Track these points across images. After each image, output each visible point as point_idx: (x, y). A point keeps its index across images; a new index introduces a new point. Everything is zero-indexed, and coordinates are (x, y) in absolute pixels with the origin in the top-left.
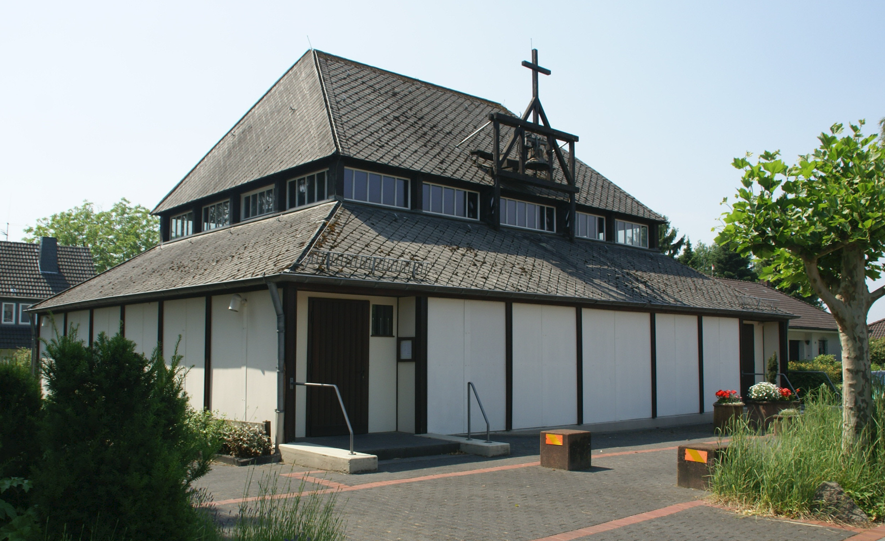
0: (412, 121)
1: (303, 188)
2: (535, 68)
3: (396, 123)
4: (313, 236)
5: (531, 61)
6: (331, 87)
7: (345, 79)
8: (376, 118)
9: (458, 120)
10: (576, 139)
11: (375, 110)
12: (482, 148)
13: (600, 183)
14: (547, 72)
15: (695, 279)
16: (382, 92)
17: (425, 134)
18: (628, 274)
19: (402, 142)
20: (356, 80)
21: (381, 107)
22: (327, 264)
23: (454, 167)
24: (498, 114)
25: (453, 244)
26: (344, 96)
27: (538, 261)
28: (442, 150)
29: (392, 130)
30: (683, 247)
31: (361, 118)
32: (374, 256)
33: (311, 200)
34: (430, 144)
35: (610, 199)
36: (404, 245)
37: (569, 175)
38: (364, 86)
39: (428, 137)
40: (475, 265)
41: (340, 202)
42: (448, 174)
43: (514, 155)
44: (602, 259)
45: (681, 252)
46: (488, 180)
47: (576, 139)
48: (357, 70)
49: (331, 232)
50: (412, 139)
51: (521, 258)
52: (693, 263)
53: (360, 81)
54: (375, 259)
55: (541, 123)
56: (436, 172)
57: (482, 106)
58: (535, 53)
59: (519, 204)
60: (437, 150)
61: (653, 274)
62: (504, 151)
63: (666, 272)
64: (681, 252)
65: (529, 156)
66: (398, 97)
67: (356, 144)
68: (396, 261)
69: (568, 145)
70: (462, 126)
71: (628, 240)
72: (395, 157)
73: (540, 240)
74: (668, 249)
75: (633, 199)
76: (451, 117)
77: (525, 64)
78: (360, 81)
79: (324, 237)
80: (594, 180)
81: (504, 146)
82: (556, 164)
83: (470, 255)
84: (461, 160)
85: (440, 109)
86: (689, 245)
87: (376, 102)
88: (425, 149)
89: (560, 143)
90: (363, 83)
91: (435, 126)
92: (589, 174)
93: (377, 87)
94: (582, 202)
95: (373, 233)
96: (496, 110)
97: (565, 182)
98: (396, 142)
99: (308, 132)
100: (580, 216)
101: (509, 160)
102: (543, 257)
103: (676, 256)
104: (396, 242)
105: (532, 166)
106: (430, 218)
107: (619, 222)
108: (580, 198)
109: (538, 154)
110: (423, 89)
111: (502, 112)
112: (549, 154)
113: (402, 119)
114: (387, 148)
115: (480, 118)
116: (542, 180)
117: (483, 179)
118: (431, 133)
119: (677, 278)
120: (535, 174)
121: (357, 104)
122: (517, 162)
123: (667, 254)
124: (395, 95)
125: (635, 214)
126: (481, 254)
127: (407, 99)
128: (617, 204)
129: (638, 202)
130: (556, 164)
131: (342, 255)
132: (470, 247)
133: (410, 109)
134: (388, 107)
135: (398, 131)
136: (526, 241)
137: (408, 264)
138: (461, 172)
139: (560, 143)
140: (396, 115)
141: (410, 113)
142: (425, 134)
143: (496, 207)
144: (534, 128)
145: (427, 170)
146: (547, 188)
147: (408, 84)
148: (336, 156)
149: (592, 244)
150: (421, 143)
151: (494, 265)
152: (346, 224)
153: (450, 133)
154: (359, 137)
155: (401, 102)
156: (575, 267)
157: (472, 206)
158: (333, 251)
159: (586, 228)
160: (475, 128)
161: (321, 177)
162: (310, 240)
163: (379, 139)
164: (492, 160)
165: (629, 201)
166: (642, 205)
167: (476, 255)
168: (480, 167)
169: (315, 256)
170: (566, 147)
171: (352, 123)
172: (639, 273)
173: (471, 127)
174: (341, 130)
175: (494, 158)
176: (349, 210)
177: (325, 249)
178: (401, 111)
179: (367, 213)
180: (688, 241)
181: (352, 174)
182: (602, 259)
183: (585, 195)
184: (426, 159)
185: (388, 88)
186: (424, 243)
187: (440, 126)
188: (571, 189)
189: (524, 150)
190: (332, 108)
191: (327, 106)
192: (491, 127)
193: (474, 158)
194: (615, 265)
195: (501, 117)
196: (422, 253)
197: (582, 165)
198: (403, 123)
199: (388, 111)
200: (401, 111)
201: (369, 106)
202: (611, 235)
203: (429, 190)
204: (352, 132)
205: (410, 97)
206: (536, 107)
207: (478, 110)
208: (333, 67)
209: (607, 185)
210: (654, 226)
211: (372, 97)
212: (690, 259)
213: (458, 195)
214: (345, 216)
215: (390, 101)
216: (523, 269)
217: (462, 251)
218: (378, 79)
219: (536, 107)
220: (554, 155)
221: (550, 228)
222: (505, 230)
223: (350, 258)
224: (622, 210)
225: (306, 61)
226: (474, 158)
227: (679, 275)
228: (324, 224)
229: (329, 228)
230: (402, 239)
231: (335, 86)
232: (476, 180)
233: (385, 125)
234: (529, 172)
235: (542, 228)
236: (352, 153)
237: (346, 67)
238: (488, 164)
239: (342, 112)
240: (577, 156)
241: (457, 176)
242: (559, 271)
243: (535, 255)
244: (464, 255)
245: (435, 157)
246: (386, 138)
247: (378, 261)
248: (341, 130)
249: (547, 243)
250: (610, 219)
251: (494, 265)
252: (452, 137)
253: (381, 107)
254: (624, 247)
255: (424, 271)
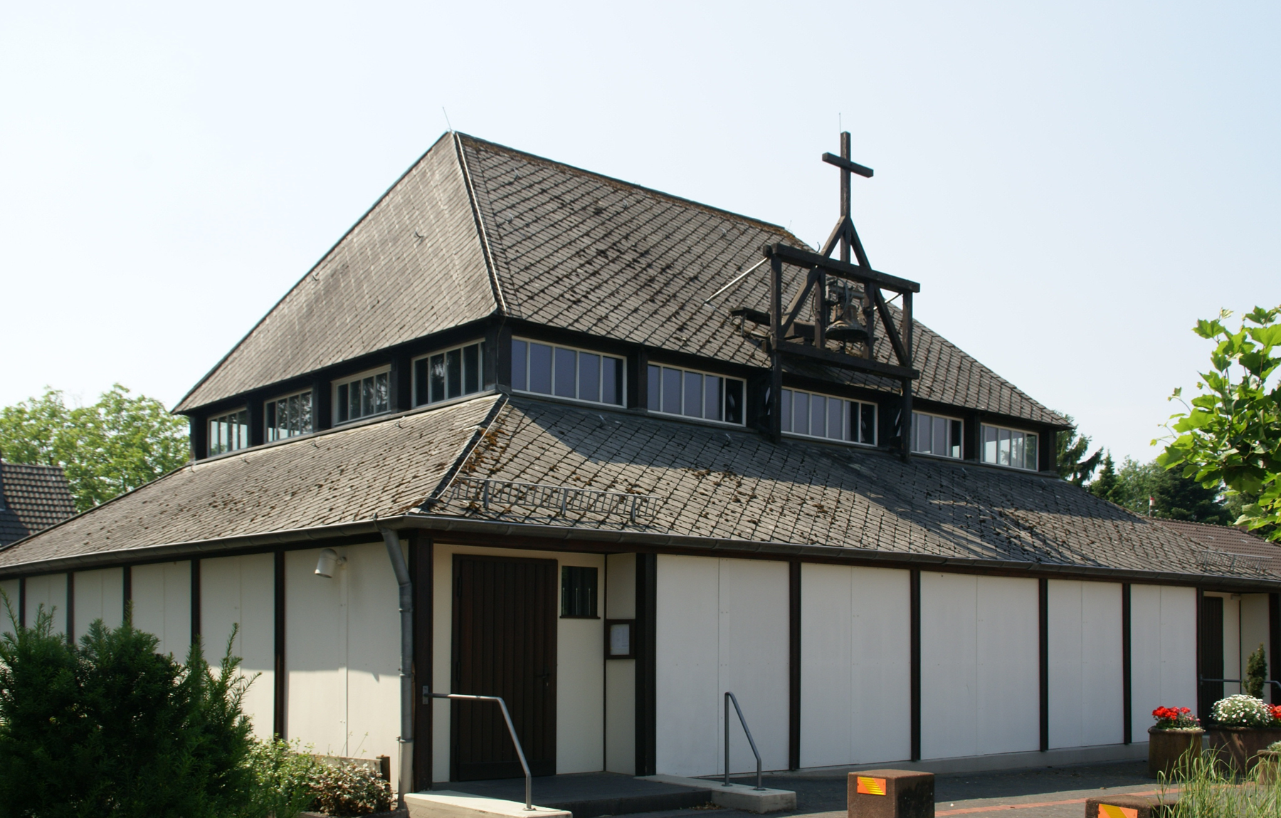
0: (628, 257)
1: (442, 371)
2: (846, 165)
3: (600, 261)
4: (459, 453)
5: (838, 153)
6: (486, 199)
7: (510, 184)
8: (566, 253)
9: (710, 255)
10: (916, 287)
11: (565, 239)
12: (751, 304)
13: (956, 362)
14: (867, 173)
15: (1119, 522)
16: (577, 207)
17: (652, 280)
18: (1001, 514)
19: (612, 294)
20: (531, 186)
21: (575, 234)
22: (484, 499)
23: (703, 337)
24: (779, 246)
25: (701, 466)
26: (510, 214)
27: (846, 494)
28: (682, 308)
29: (594, 274)
30: (1100, 468)
31: (540, 253)
32: (565, 486)
33: (455, 392)
34: (660, 297)
35: (973, 390)
36: (615, 467)
37: (903, 350)
38: (545, 198)
39: (656, 286)
40: (738, 501)
41: (504, 395)
42: (692, 349)
43: (807, 316)
44: (956, 490)
45: (1096, 476)
46: (762, 359)
47: (916, 287)
48: (531, 169)
49: (491, 445)
50: (629, 289)
51: (816, 489)
52: (1117, 494)
53: (537, 188)
54: (566, 491)
55: (854, 261)
56: (671, 346)
57: (751, 231)
58: (846, 139)
59: (814, 399)
60: (673, 307)
61: (1045, 515)
62: (790, 309)
63: (1069, 511)
64: (1096, 476)
65: (833, 317)
66: (605, 215)
67: (531, 298)
68: (603, 495)
69: (901, 298)
70: (716, 266)
71: (1002, 456)
72: (599, 320)
73: (850, 459)
74: (1072, 470)
75: (1013, 389)
76: (698, 250)
77: (829, 158)
78: (537, 188)
79: (479, 455)
80: (945, 358)
81: (789, 301)
82: (880, 331)
83: (730, 484)
84: (714, 325)
85: (678, 236)
86: (1109, 463)
87: (565, 224)
88: (651, 307)
89: (887, 295)
90: (544, 191)
91: (668, 267)
92: (936, 347)
93: (568, 198)
94: (923, 394)
95: (563, 448)
96: (775, 240)
97: (894, 361)
98: (601, 293)
99: (447, 276)
100: (920, 420)
101: (797, 325)
102: (854, 488)
103: (1086, 483)
104: (602, 463)
105: (836, 334)
106: (660, 423)
107: (986, 428)
108: (920, 388)
109: (848, 313)
110: (648, 202)
111: (786, 243)
112: (868, 313)
113: (612, 254)
114: (586, 304)
115: (747, 252)
116: (855, 357)
117: (752, 356)
118: (662, 279)
119: (1088, 521)
120: (843, 348)
121: (534, 228)
122: (812, 327)
123: (1070, 478)
124: (598, 212)
125: (1015, 413)
126: (748, 483)
127: (620, 220)
128: (984, 398)
129: (1021, 395)
130: (880, 331)
131: (509, 485)
132: (729, 471)
133: (626, 238)
134: (587, 234)
135: (605, 275)
136: (825, 461)
137: (623, 499)
138: (715, 345)
139: (887, 295)
140: (602, 247)
141: (626, 244)
142: (652, 280)
143: (775, 405)
144: (842, 269)
145: (655, 341)
146: (863, 371)
147: (621, 194)
148: (497, 317)
149: (939, 465)
150: (644, 295)
151: (770, 500)
152: (515, 433)
153: (696, 278)
154: (537, 285)
155: (610, 225)
156: (910, 504)
157: (733, 402)
158: (494, 477)
159: (930, 438)
160: (739, 269)
161: (471, 352)
162: (454, 460)
163: (572, 289)
164: (768, 324)
165: (1006, 392)
166: (1028, 399)
167: (739, 485)
168: (747, 336)
169: (463, 486)
170: (898, 302)
171: (524, 261)
172: (1021, 513)
173: (731, 269)
174: (504, 273)
175: (773, 321)
176: (521, 409)
177: (480, 475)
178: (610, 241)
179: (552, 414)
180: (1108, 458)
181: (525, 348)
182: (956, 490)
183: (928, 383)
184: (653, 323)
185: (587, 200)
186: (651, 464)
187: (678, 267)
188: (906, 373)
189: (825, 307)
190: (488, 235)
191: (480, 232)
192: (768, 267)
193: (737, 321)
194: (977, 497)
195: (784, 251)
196: (646, 482)
197: (924, 331)
198: (613, 261)
199: (587, 241)
200: (610, 241)
201: (554, 231)
202: (973, 450)
203: (659, 376)
204: (525, 277)
205: (626, 216)
206: (846, 233)
207: (744, 239)
208: (490, 163)
209: (967, 365)
210: (1049, 435)
211: (558, 216)
212: (1110, 487)
213: (709, 383)
214: (513, 419)
215: (590, 224)
216: (820, 507)
217: (714, 477)
218: (570, 185)
219: (846, 233)
220: (877, 315)
221: (868, 437)
222: (790, 443)
223: (524, 490)
224: (994, 408)
225: (442, 153)
226: (737, 321)
227: (1091, 516)
228: (479, 434)
229: (486, 439)
230: (612, 457)
231: (493, 196)
232: (740, 359)
233: (582, 265)
234: (833, 345)
235: (854, 438)
236: (526, 312)
237: (513, 164)
238: (761, 331)
239: (507, 242)
240: (916, 315)
241: (708, 352)
242: (881, 511)
243: (840, 485)
244: (718, 485)
245: (669, 319)
246: (584, 287)
247: (572, 494)
248: (504, 273)
249: (862, 462)
250: (971, 423)
251: (770, 500)
252: (697, 284)
253: (575, 234)
254: (996, 468)
255: (650, 512)
